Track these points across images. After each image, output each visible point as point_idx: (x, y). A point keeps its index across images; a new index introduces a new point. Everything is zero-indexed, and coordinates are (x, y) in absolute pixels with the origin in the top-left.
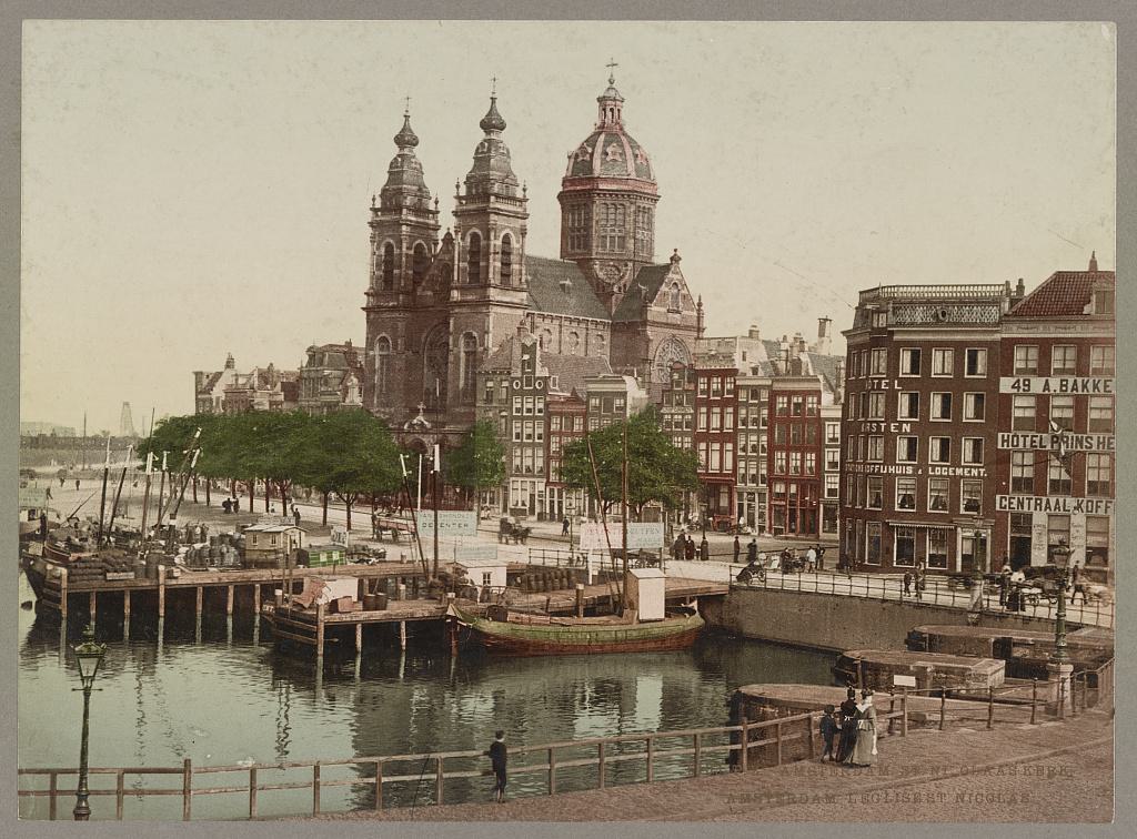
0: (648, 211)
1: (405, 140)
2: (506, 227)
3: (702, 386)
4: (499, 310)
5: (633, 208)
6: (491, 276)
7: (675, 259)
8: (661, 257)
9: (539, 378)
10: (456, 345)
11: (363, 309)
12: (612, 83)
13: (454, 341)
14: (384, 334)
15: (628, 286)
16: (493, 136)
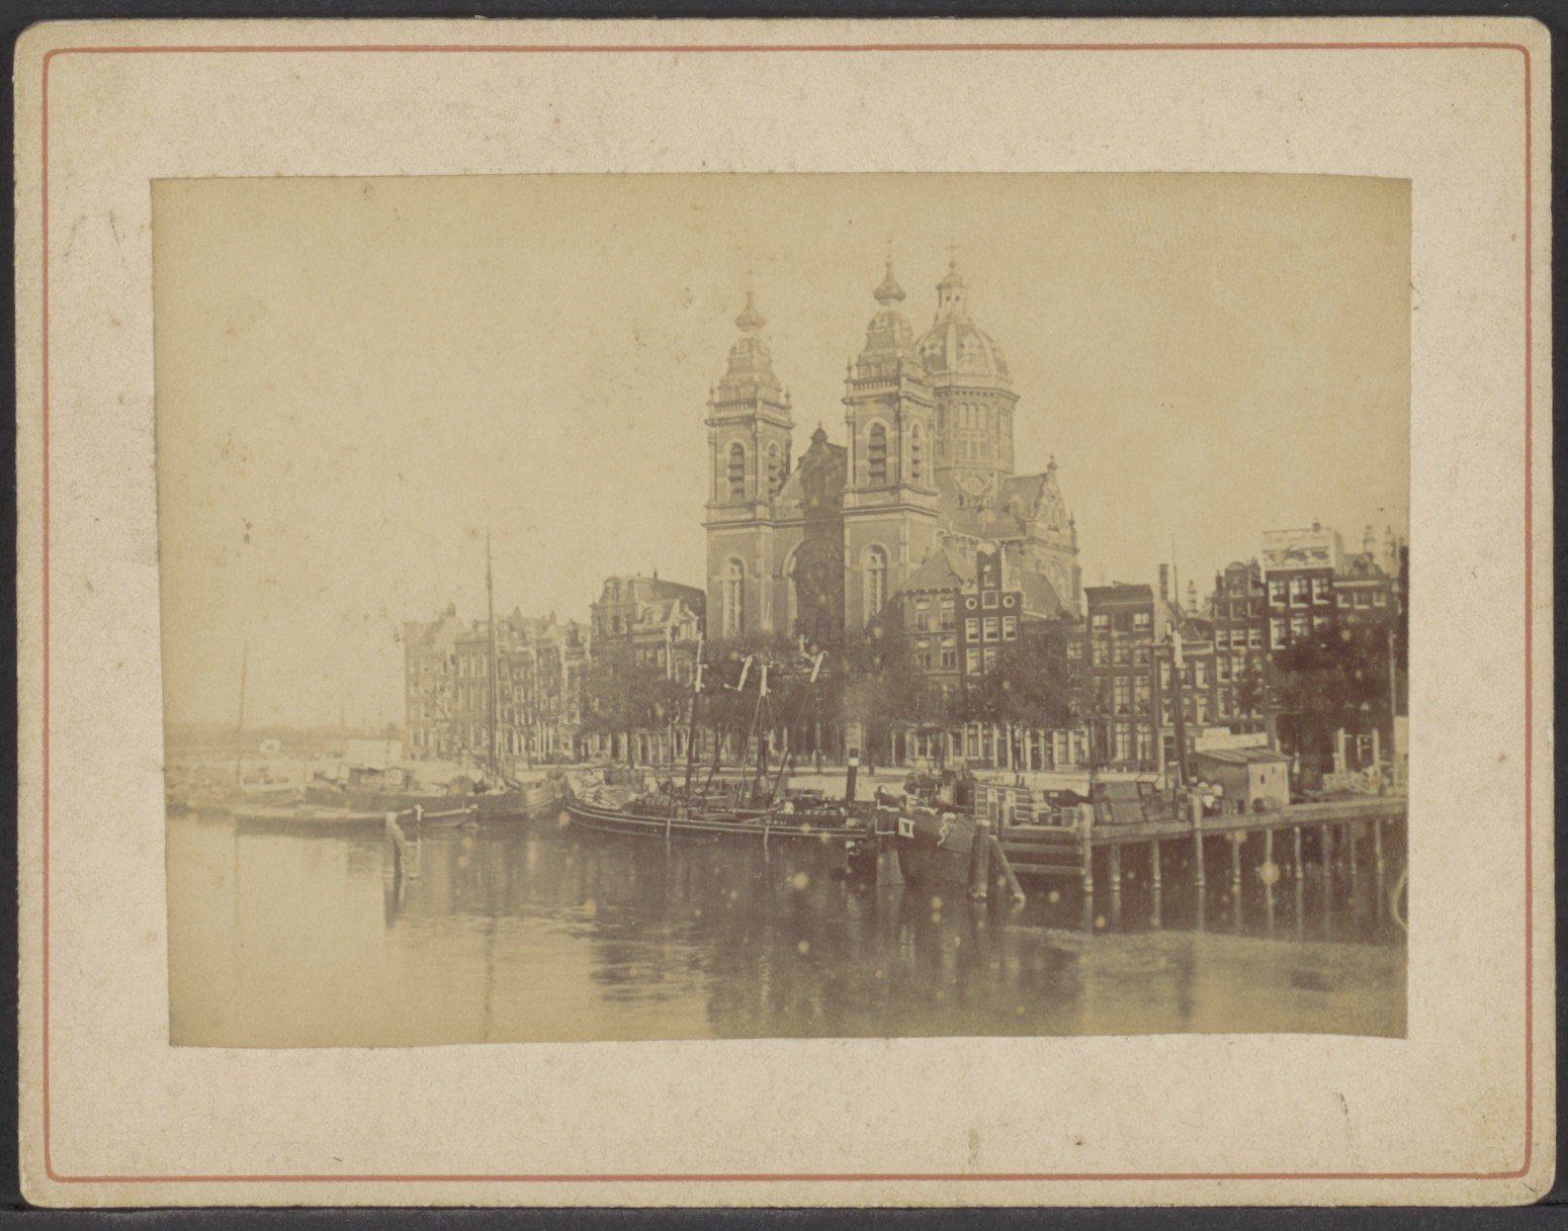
0: (1008, 413)
1: (749, 321)
2: (917, 417)
3: (1273, 592)
4: (917, 517)
5: (994, 411)
6: (904, 474)
7: (1052, 467)
8: (1027, 465)
9: (1008, 594)
10: (855, 559)
11: (703, 525)
12: (952, 266)
13: (852, 557)
14: (734, 555)
15: (995, 499)
16: (894, 306)
